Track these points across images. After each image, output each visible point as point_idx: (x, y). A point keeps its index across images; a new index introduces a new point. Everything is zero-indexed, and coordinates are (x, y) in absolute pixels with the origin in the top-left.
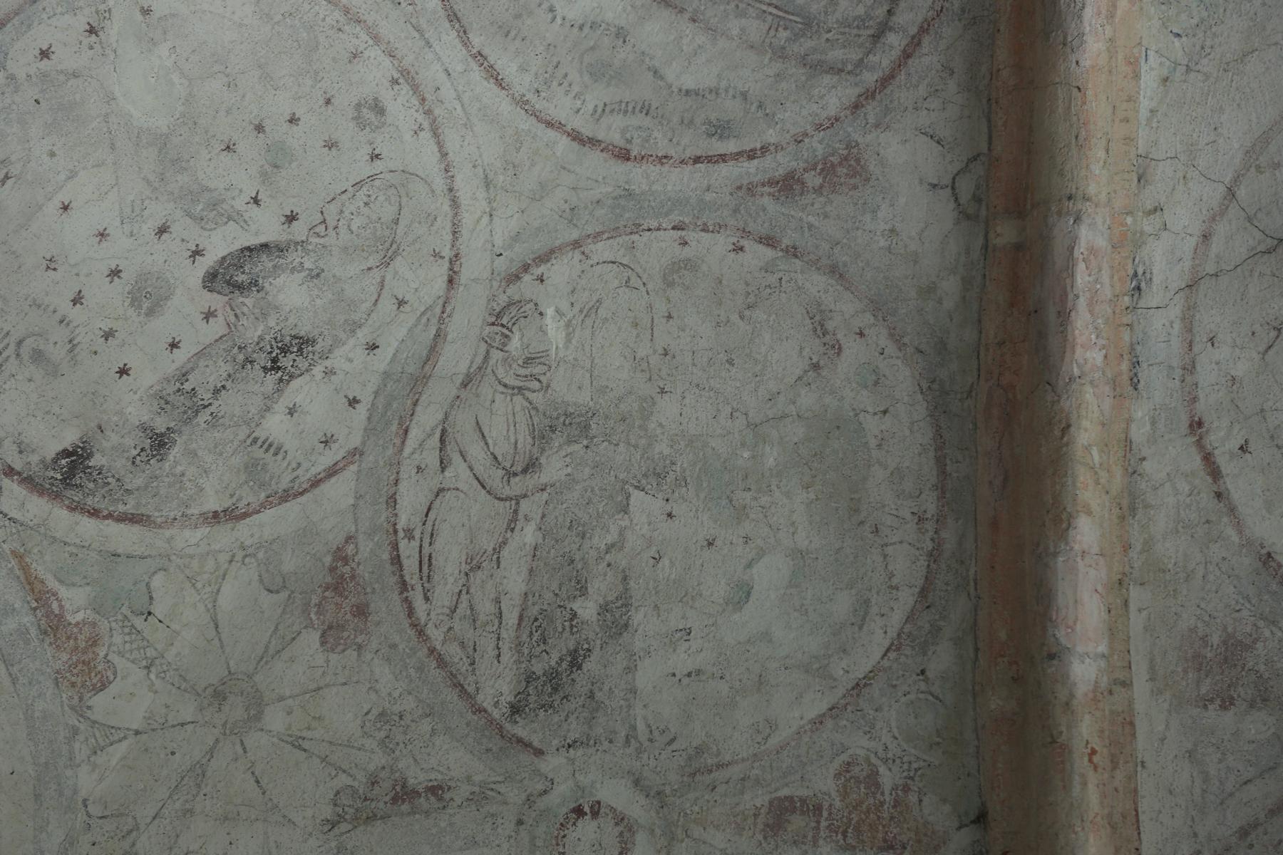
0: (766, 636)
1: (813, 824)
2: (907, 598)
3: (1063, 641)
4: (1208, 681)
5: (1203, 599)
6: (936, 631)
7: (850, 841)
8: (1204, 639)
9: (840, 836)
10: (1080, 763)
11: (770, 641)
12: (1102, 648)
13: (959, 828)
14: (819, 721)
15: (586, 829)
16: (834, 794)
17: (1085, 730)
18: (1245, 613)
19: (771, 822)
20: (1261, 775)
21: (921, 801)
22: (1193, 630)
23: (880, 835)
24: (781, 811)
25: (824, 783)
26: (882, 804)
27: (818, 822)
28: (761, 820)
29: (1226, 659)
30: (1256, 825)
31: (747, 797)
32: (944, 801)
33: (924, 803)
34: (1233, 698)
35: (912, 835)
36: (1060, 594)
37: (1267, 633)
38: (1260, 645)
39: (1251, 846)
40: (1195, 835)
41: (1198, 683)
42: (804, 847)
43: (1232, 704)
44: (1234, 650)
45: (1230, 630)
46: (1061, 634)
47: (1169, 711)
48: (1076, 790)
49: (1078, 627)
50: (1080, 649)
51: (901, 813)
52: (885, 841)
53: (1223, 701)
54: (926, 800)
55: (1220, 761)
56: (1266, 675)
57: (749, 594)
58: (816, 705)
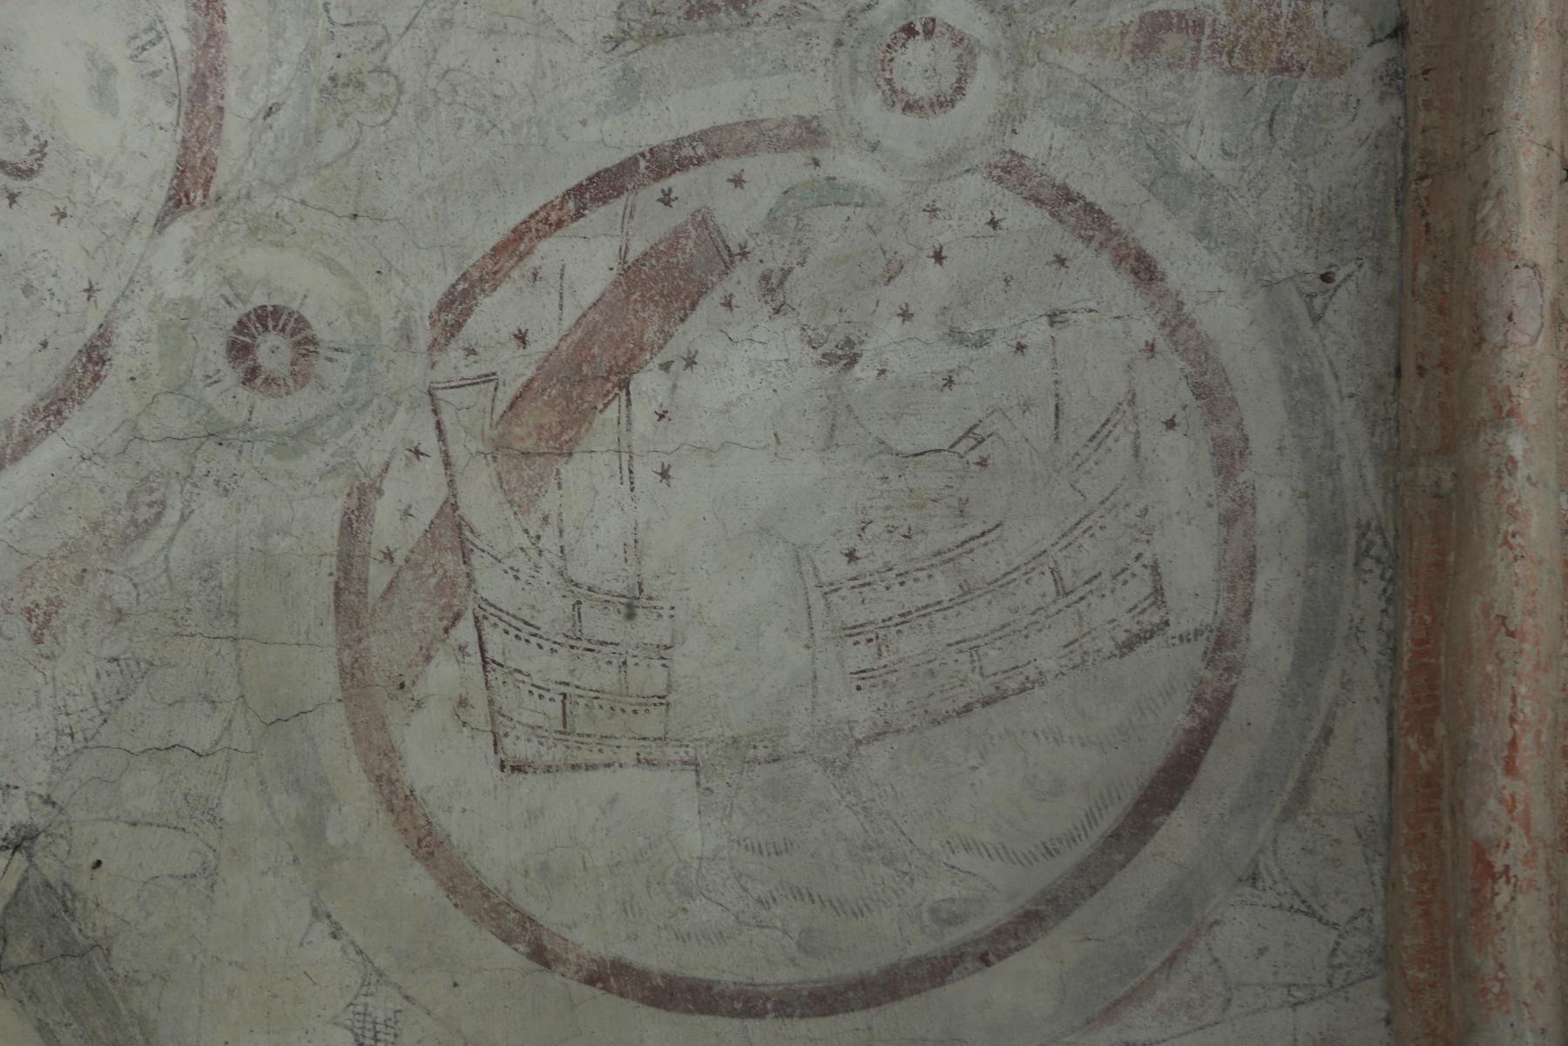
1: (1193, 44)
7: (1236, 62)
9: (1224, 58)
13: (1371, 44)
15: (918, 52)
16: (1219, 6)
19: (1141, 41)
21: (1325, 13)
23: (1274, 55)
24: (1155, 27)
26: (1278, 17)
27: (1199, 41)
28: (1128, 40)
31: (1113, 12)
32: (1355, 11)
33: (1330, 15)
35: (1313, 54)
42: (1180, 72)
51: (1301, 28)
52: (1279, 61)
54: (1332, 12)
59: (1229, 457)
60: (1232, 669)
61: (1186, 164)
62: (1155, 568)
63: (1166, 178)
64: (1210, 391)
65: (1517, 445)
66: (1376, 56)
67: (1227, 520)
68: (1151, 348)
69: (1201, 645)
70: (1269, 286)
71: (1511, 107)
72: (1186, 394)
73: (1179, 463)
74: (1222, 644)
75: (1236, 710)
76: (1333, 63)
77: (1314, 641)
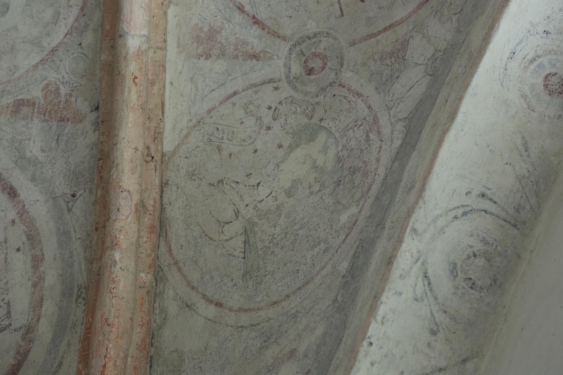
0: (16, 28)
1: (32, 111)
2: (75, 11)
3: (125, 29)
4: (202, 47)
5: (202, 11)
6: (87, 25)
7: (46, 118)
8: (201, 29)
9: (42, 116)
10: (129, 82)
11: (17, 30)
12: (145, 32)
13: (91, 112)
14: (36, 66)
16: (41, 98)
17: (132, 68)
18: (219, 17)
19: (14, 110)
20: (219, 88)
21: (76, 100)
22: (197, 25)
23: (59, 115)
24: (19, 104)
25: (37, 93)
26: (60, 102)
27: (34, 110)
28: (10, 109)
29: (209, 37)
30: (214, 109)
31: (4, 99)
32: (86, 100)
33: (78, 101)
34: (210, 54)
35: (72, 115)
36: (125, 9)
37: (227, 26)
38: (223, 31)
39: (211, 117)
40: (190, 113)
41: (197, 48)
42: (27, 121)
43: (210, 57)
44: (213, 33)
45: (212, 25)
46: (125, 26)
47: (184, 61)
48: (126, 94)
49: (132, 23)
50: (132, 33)
51: (68, 106)
52: (61, 117)
53: (207, 56)
54: (78, 100)
55: (203, 82)
56: (225, 44)
57: (8, 9)
58: (35, 59)
59: (37, 261)
60: (31, 341)
61: (28, 154)
62: (8, 304)
63: (22, 160)
64: (33, 238)
65: (117, 256)
66: (93, 116)
67: (35, 285)
68: (13, 222)
69: (22, 331)
70: (54, 199)
71: (122, 135)
72: (24, 238)
73: (20, 263)
74: (28, 332)
75: (30, 357)
76: (79, 119)
77: (60, 329)
